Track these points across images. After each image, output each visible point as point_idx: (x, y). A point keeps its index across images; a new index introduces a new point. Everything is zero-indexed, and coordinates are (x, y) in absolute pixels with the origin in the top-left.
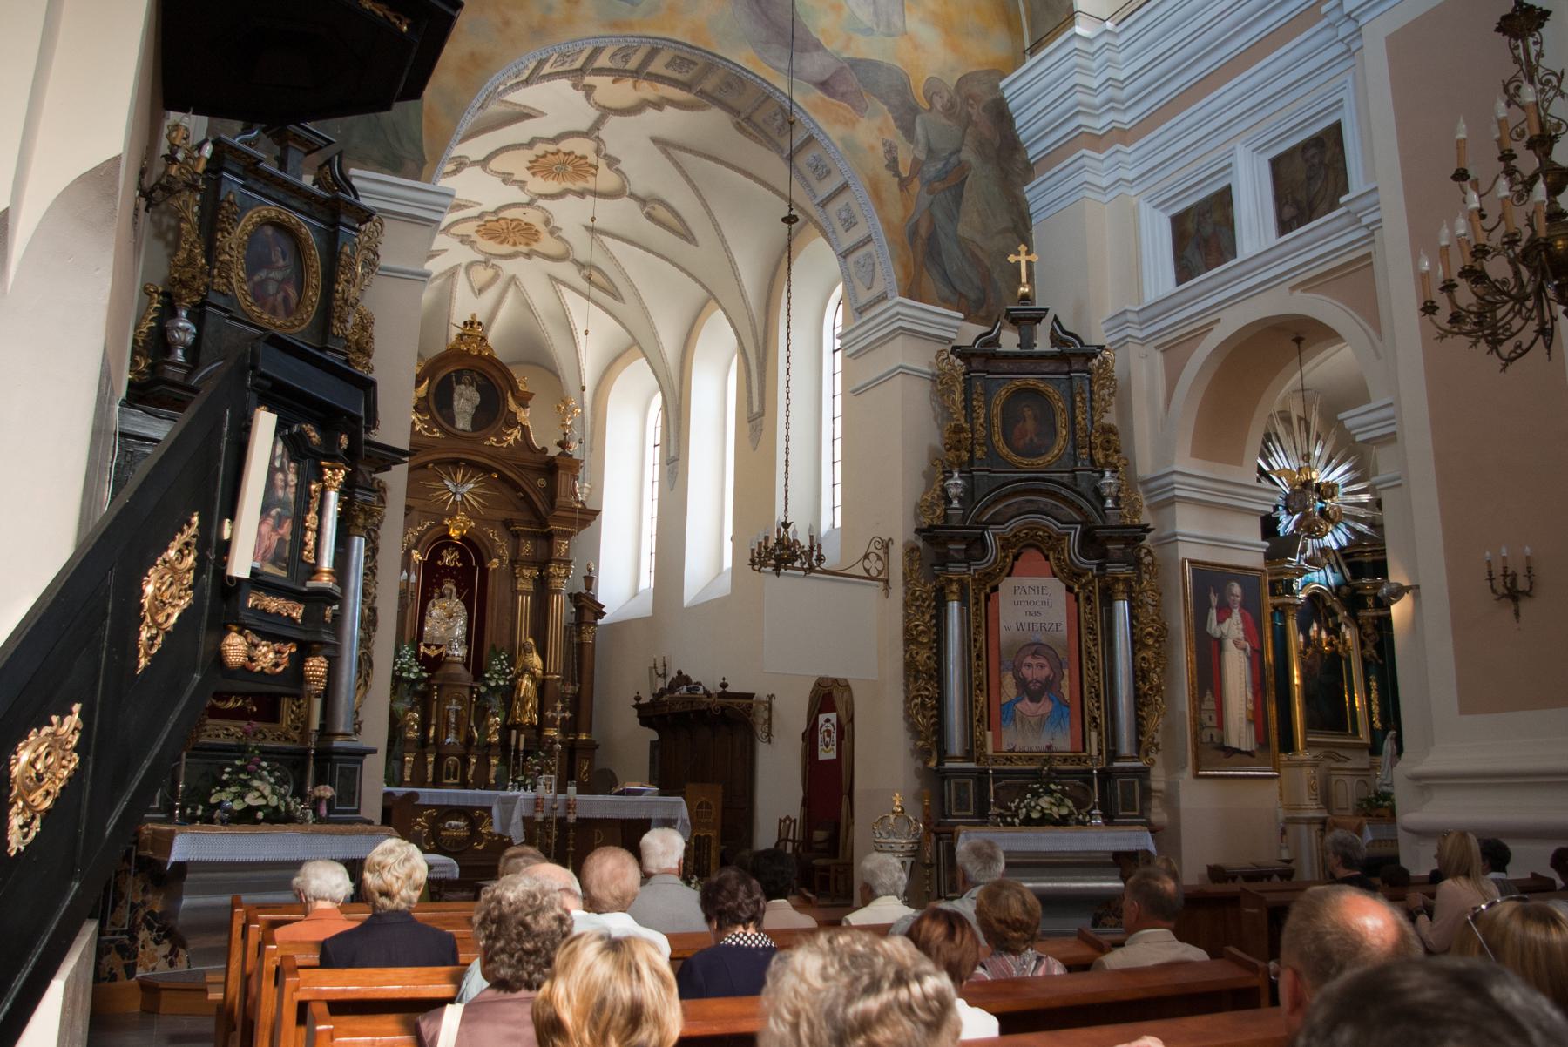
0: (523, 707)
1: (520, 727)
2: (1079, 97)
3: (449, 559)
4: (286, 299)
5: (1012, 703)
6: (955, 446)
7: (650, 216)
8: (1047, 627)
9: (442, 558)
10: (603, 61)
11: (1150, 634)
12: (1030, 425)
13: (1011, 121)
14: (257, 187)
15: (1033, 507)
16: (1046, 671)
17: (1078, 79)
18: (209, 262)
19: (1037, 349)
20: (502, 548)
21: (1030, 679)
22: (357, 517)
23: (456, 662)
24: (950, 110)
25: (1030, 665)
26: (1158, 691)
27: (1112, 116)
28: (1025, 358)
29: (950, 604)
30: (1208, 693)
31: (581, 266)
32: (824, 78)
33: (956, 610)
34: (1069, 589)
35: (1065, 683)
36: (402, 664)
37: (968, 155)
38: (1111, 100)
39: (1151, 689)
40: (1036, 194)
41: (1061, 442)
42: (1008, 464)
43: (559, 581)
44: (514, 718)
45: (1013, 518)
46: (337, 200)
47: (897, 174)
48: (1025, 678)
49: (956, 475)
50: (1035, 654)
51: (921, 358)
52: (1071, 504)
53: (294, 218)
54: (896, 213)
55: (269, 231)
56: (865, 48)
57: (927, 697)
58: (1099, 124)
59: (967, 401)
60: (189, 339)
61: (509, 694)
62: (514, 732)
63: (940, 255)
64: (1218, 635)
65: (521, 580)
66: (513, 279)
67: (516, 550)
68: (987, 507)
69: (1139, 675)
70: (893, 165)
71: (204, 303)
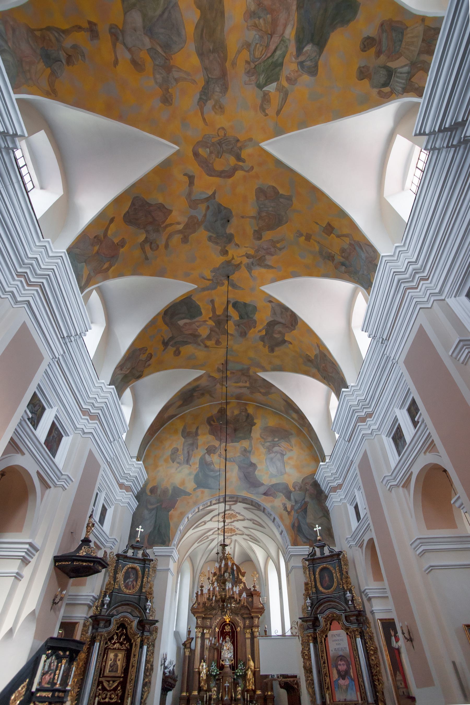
0: (249, 683)
1: (248, 691)
2: (327, 479)
3: (228, 629)
4: (133, 585)
5: (337, 680)
6: (307, 589)
7: (254, 523)
8: (343, 649)
9: (225, 629)
10: (214, 502)
11: (372, 649)
12: (327, 578)
13: (319, 485)
14: (127, 561)
15: (331, 606)
16: (345, 667)
17: (325, 475)
18: (115, 582)
19: (325, 555)
20: (241, 624)
21: (341, 670)
22: (145, 640)
23: (228, 667)
24: (301, 489)
25: (340, 665)
26: (379, 673)
27: (336, 482)
28: (323, 558)
29: (310, 644)
30: (398, 672)
31: (248, 535)
32: (265, 492)
33: (312, 646)
34: (347, 634)
35: (351, 671)
36: (212, 669)
37: (307, 499)
38: (334, 478)
39: (376, 672)
40: (328, 504)
41: (335, 584)
42: (322, 593)
43: (256, 633)
44: (247, 687)
45: (325, 611)
46: (144, 559)
47: (287, 511)
48: (339, 670)
49: (308, 599)
50: (341, 660)
51: (298, 563)
52: (341, 605)
53: (136, 565)
54: (288, 522)
55: (130, 570)
56: (274, 481)
57: (310, 680)
58: (335, 484)
59: (309, 574)
60: (108, 602)
61: (244, 676)
62: (246, 693)
63: (302, 530)
64: (397, 647)
65: (247, 634)
66: (236, 540)
67: (244, 624)
68: (317, 608)
69: (370, 666)
70: (285, 509)
71: (112, 592)
